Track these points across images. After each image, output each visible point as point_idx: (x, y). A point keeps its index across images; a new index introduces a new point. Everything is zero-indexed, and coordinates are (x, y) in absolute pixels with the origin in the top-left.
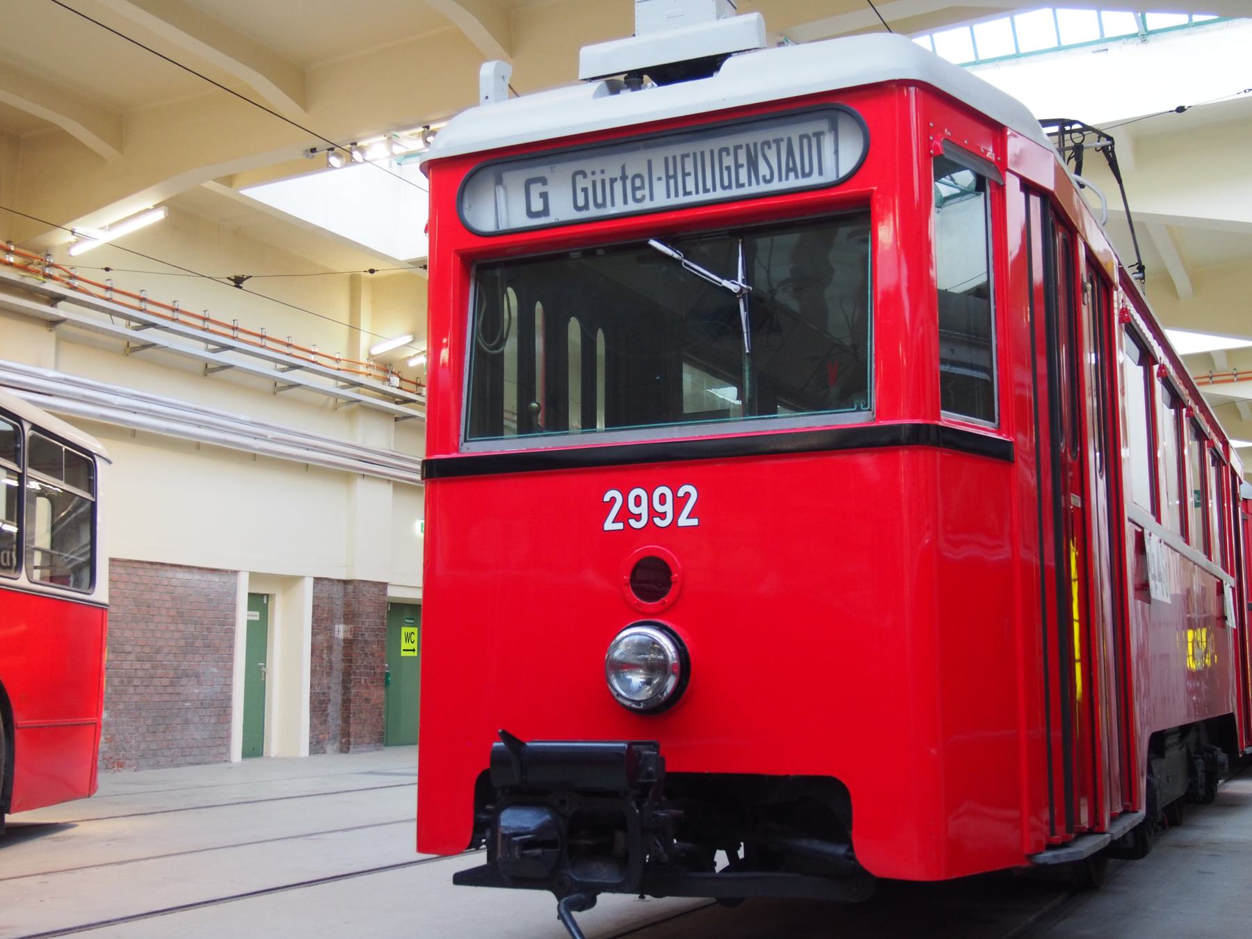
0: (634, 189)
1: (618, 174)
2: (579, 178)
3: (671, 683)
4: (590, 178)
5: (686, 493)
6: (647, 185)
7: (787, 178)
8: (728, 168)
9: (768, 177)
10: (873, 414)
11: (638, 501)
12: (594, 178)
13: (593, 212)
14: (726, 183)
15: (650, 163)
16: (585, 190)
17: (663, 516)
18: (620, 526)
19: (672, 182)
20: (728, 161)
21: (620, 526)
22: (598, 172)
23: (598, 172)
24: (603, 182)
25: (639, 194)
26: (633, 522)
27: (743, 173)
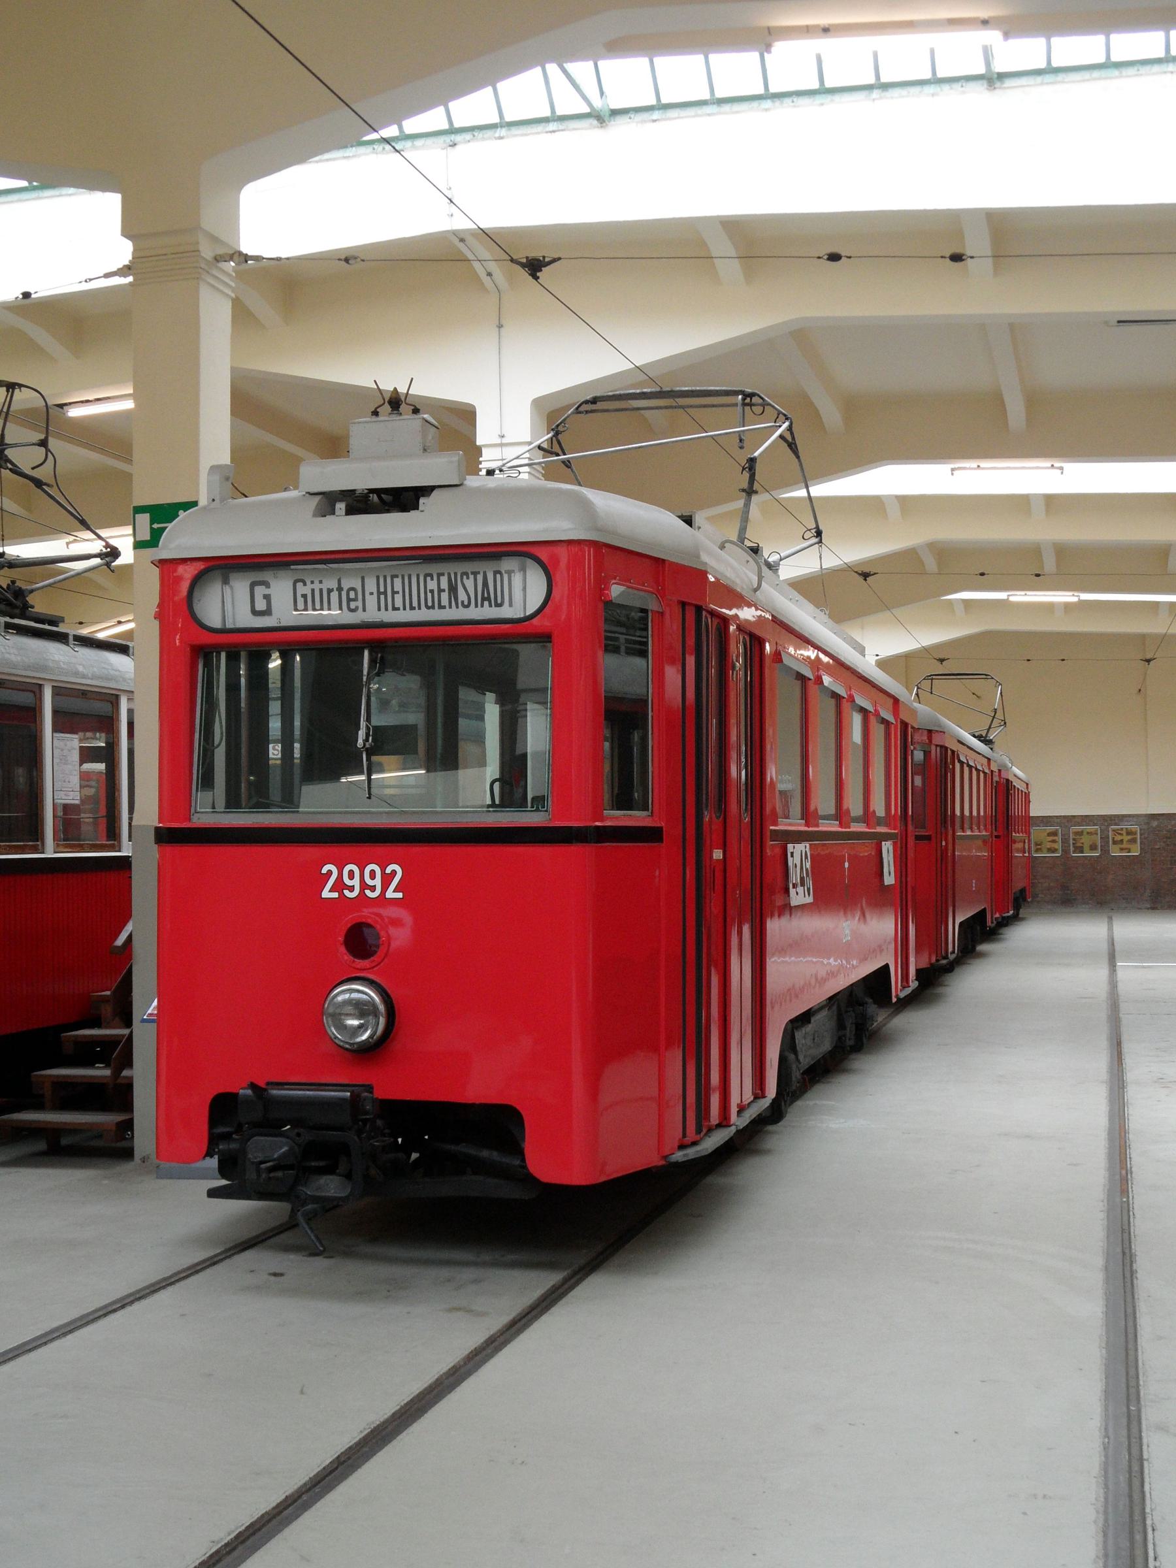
0: (349, 600)
1: (333, 584)
2: (299, 585)
4: (309, 586)
5: (394, 870)
6: (360, 597)
7: (482, 606)
8: (432, 591)
9: (466, 603)
10: (549, 815)
11: (351, 875)
12: (312, 586)
14: (430, 604)
15: (363, 579)
16: (304, 596)
17: (373, 888)
18: (335, 895)
19: (382, 597)
20: (432, 585)
21: (335, 895)
22: (316, 582)
23: (316, 582)
24: (321, 590)
25: (353, 605)
26: (346, 892)
27: (445, 597)
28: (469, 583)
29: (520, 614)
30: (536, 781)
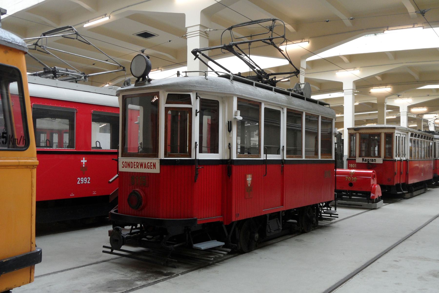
17: (85, 182)
18: (80, 183)
21: (80, 183)
26: (81, 183)
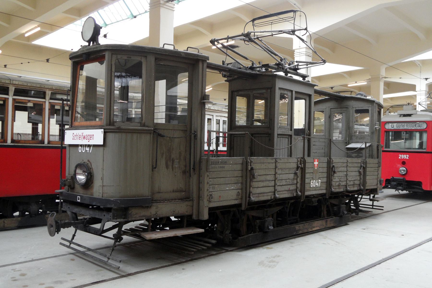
1: (401, 125)
3: (406, 172)
11: (402, 156)
13: (398, 128)
17: (405, 157)
18: (401, 158)
20: (413, 125)
21: (401, 158)
27: (414, 126)
28: (417, 125)
29: (423, 128)
30: (425, 146)
